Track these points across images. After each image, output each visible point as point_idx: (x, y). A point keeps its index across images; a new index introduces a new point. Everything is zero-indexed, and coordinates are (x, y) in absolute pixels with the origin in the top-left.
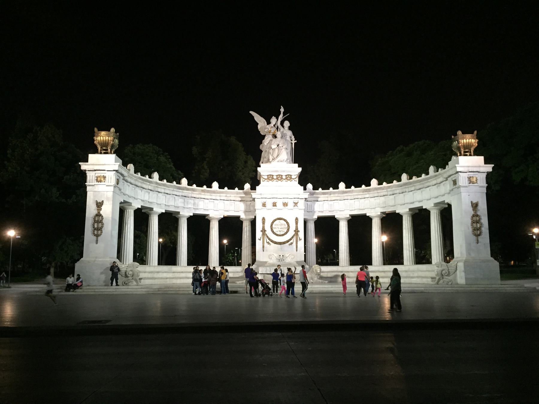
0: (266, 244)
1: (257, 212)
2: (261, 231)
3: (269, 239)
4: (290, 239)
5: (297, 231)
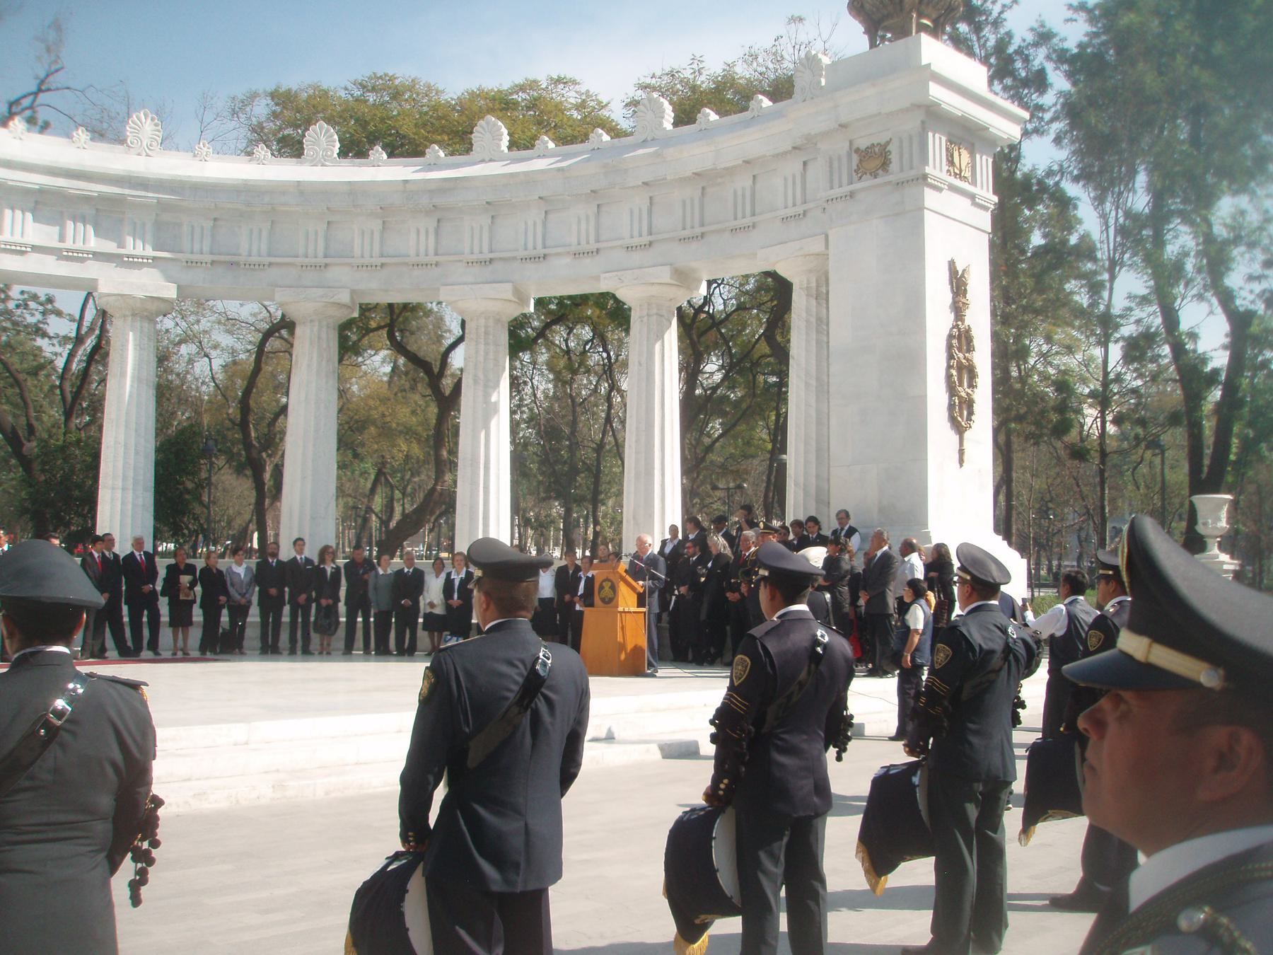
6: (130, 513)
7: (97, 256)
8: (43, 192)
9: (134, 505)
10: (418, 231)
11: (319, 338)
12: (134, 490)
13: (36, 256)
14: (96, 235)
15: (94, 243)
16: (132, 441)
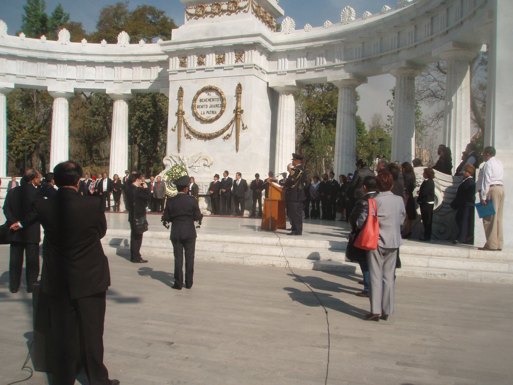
0: (183, 138)
1: (171, 78)
2: (177, 114)
3: (189, 129)
4: (228, 127)
5: (238, 112)
6: (340, 165)
7: (327, 68)
8: (307, 49)
9: (342, 162)
10: (426, 25)
11: (400, 84)
12: (342, 156)
13: (308, 73)
14: (327, 60)
15: (325, 63)
16: (341, 137)
